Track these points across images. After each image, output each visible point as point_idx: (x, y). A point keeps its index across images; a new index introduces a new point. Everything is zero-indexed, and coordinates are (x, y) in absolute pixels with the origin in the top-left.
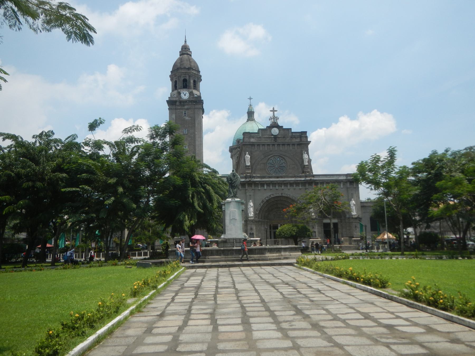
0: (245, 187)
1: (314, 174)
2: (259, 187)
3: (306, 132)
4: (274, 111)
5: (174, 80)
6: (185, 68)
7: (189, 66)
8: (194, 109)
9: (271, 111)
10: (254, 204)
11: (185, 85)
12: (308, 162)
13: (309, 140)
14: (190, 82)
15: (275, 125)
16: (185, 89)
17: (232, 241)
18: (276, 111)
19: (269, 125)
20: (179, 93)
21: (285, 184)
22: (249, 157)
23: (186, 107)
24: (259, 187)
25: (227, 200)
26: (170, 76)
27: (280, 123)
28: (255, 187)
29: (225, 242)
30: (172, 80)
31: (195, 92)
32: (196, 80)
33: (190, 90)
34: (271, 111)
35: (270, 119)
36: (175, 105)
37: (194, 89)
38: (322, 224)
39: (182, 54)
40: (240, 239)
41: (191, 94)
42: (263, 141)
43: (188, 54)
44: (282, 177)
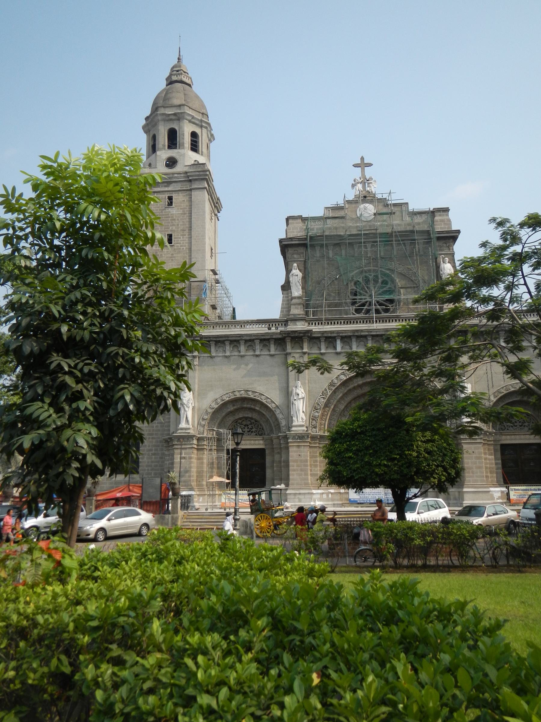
0: (284, 349)
2: (323, 346)
3: (446, 210)
4: (363, 165)
5: (151, 136)
9: (356, 166)
10: (310, 393)
13: (454, 228)
15: (367, 197)
18: (370, 165)
19: (351, 197)
22: (300, 275)
24: (323, 346)
27: (378, 189)
28: (310, 348)
32: (198, 130)
34: (356, 166)
35: (353, 186)
38: (499, 447)
39: (170, 82)
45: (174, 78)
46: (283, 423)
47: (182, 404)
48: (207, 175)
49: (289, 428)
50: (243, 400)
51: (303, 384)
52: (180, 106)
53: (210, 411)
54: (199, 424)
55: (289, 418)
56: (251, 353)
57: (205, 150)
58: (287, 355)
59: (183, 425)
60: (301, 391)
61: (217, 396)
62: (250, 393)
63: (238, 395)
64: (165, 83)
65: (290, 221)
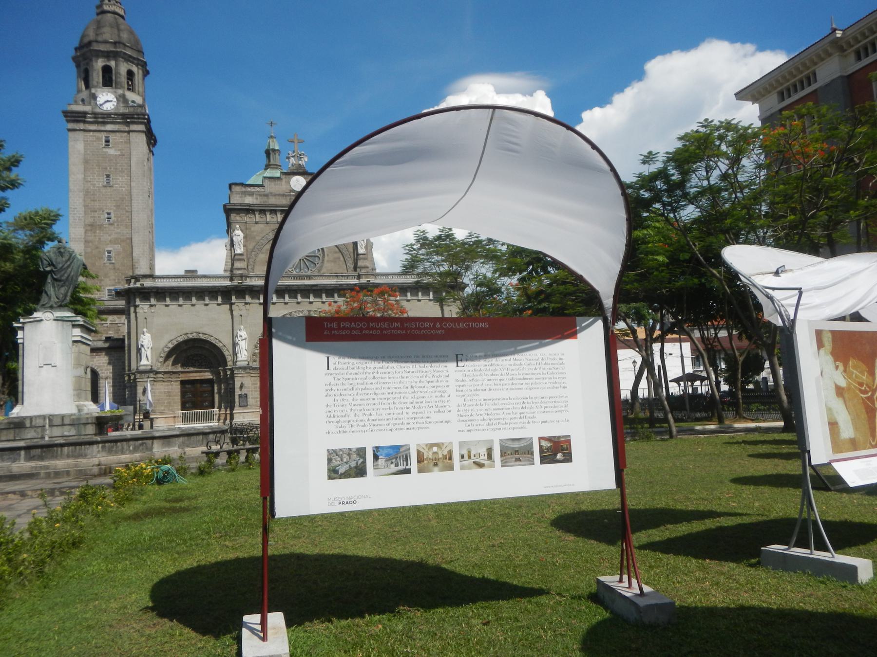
1: (378, 271)
5: (83, 68)
6: (106, 42)
7: (117, 40)
8: (129, 132)
10: (250, 335)
11: (108, 80)
12: (366, 248)
14: (118, 73)
16: (106, 89)
17: (39, 422)
20: (94, 97)
21: (317, 291)
22: (242, 235)
23: (109, 127)
25: (35, 315)
26: (74, 59)
29: (19, 425)
30: (78, 66)
31: (131, 96)
32: (135, 69)
33: (120, 92)
36: (85, 122)
37: (129, 89)
40: (63, 417)
41: (122, 99)
42: (272, 201)
43: (115, 13)
44: (309, 277)
45: (106, 8)
46: (229, 358)
47: (142, 346)
48: (145, 119)
49: (235, 363)
50: (194, 340)
51: (245, 328)
52: (115, 43)
53: (167, 350)
54: (157, 360)
55: (235, 354)
56: (202, 302)
57: (141, 90)
58: (231, 304)
59: (144, 362)
60: (243, 333)
61: (172, 338)
62: (201, 335)
63: (191, 336)
64: (95, 11)
65: (233, 187)
